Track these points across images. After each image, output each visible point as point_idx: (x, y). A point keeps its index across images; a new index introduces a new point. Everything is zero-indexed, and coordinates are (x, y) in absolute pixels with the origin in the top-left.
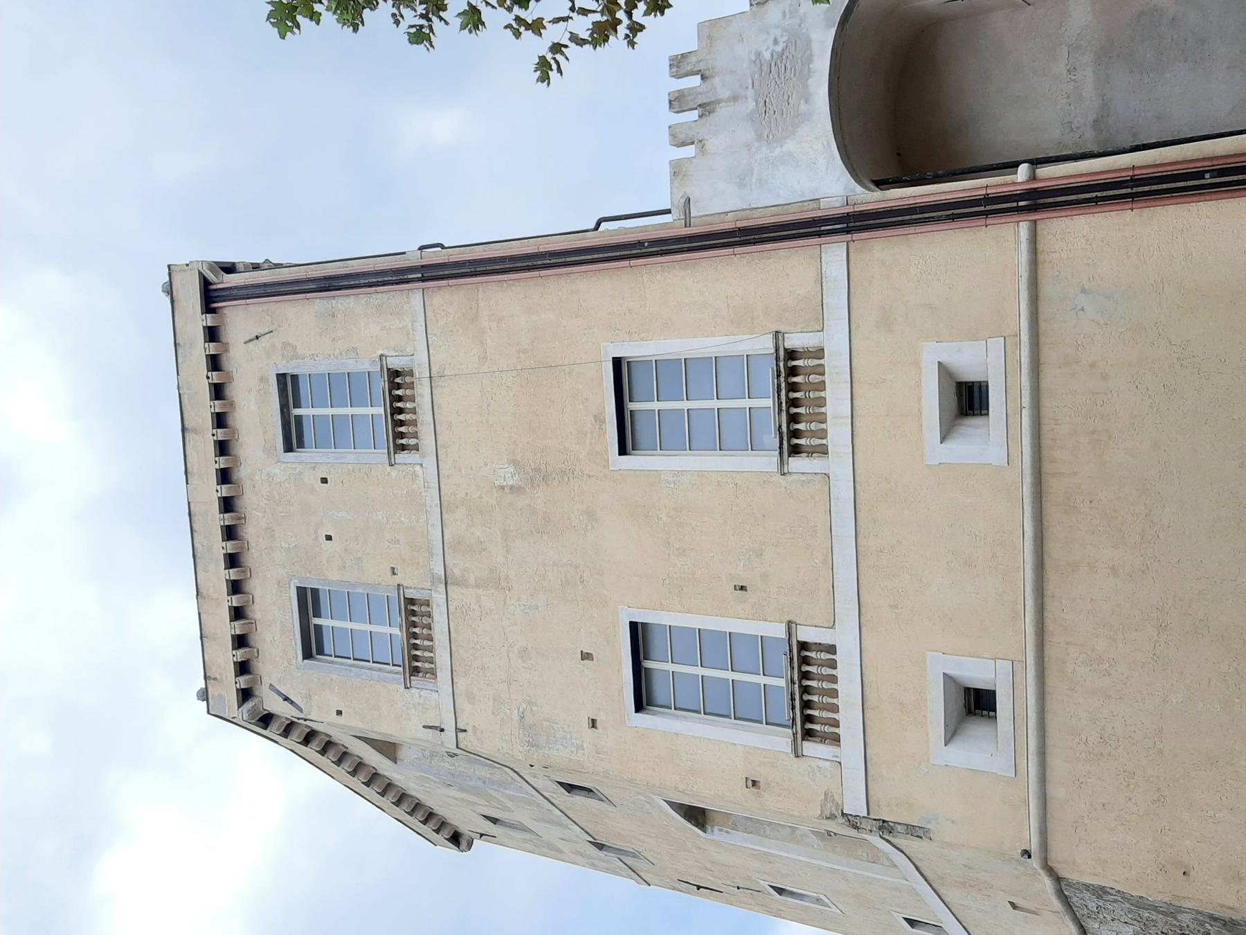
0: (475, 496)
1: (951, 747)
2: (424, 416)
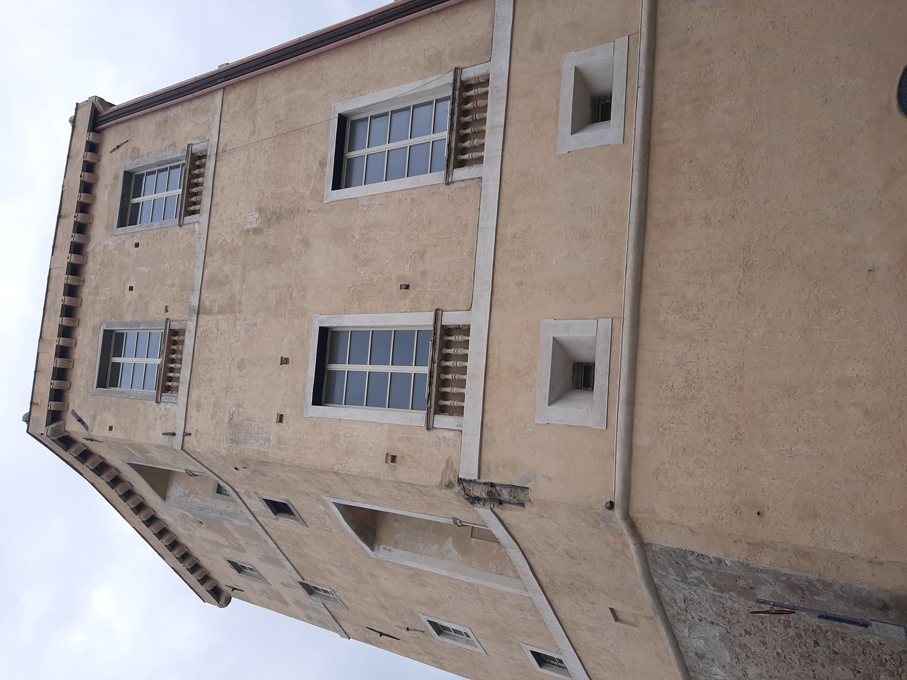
0: (229, 240)
1: (553, 407)
2: (208, 184)
